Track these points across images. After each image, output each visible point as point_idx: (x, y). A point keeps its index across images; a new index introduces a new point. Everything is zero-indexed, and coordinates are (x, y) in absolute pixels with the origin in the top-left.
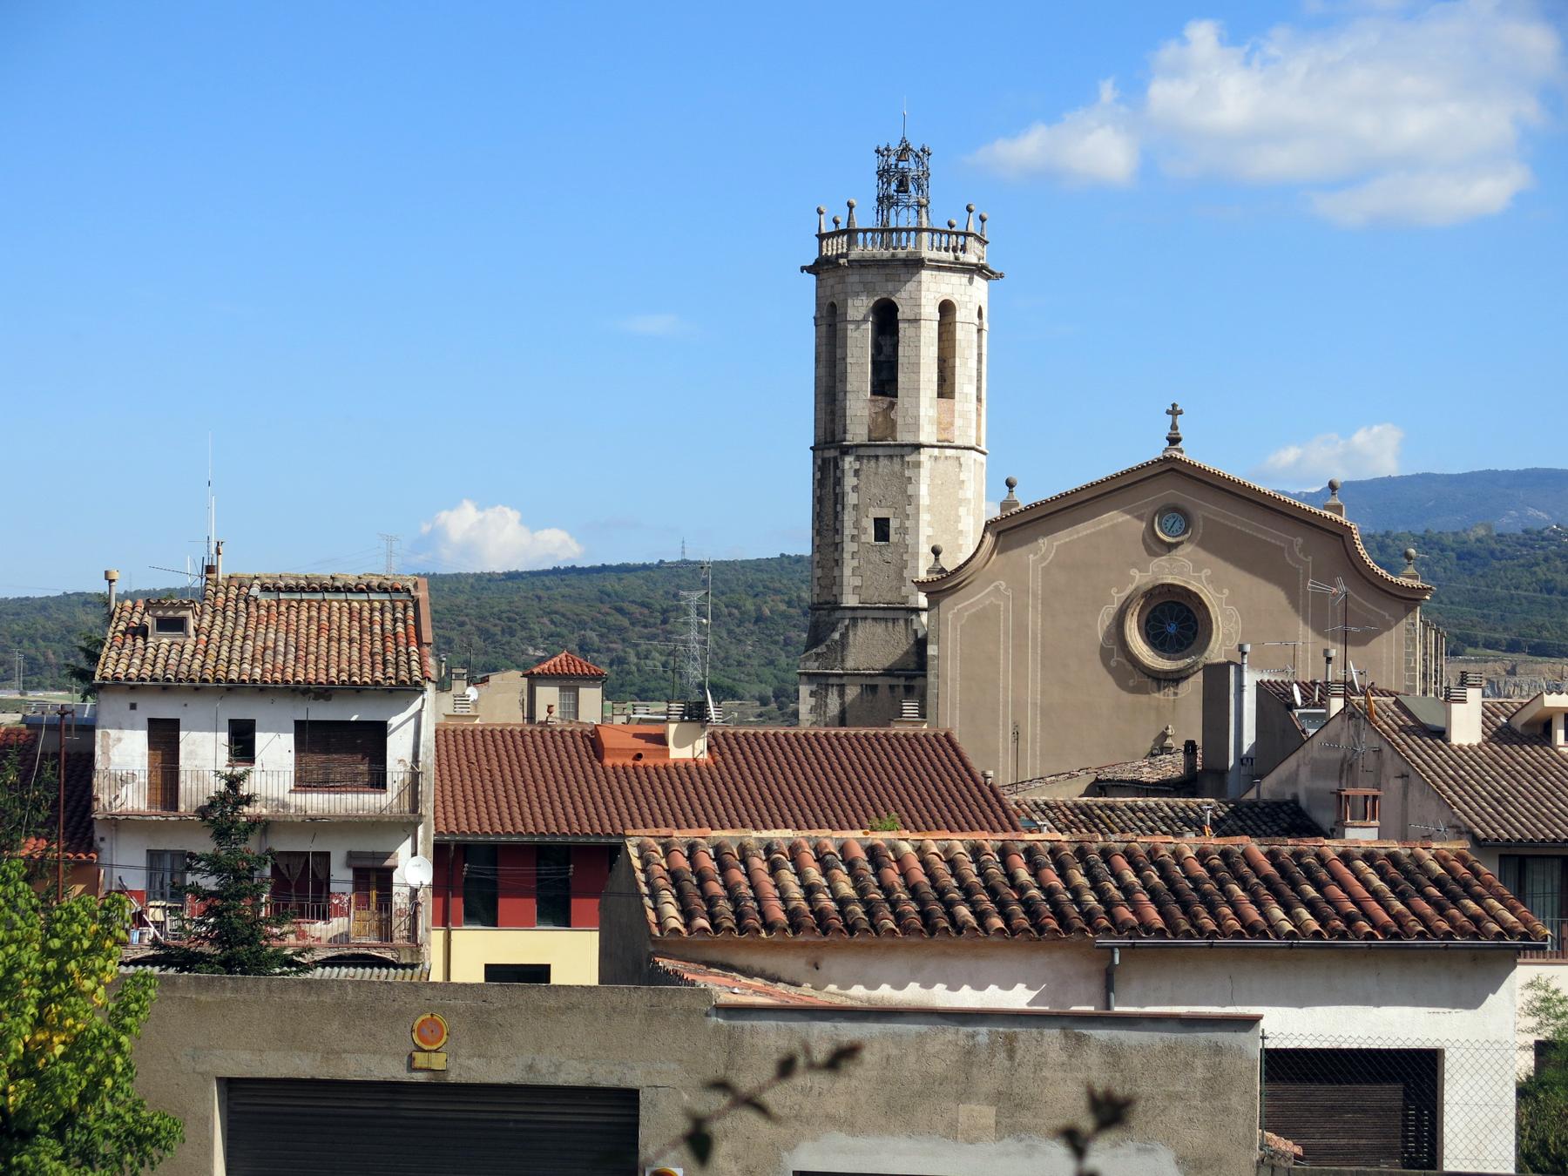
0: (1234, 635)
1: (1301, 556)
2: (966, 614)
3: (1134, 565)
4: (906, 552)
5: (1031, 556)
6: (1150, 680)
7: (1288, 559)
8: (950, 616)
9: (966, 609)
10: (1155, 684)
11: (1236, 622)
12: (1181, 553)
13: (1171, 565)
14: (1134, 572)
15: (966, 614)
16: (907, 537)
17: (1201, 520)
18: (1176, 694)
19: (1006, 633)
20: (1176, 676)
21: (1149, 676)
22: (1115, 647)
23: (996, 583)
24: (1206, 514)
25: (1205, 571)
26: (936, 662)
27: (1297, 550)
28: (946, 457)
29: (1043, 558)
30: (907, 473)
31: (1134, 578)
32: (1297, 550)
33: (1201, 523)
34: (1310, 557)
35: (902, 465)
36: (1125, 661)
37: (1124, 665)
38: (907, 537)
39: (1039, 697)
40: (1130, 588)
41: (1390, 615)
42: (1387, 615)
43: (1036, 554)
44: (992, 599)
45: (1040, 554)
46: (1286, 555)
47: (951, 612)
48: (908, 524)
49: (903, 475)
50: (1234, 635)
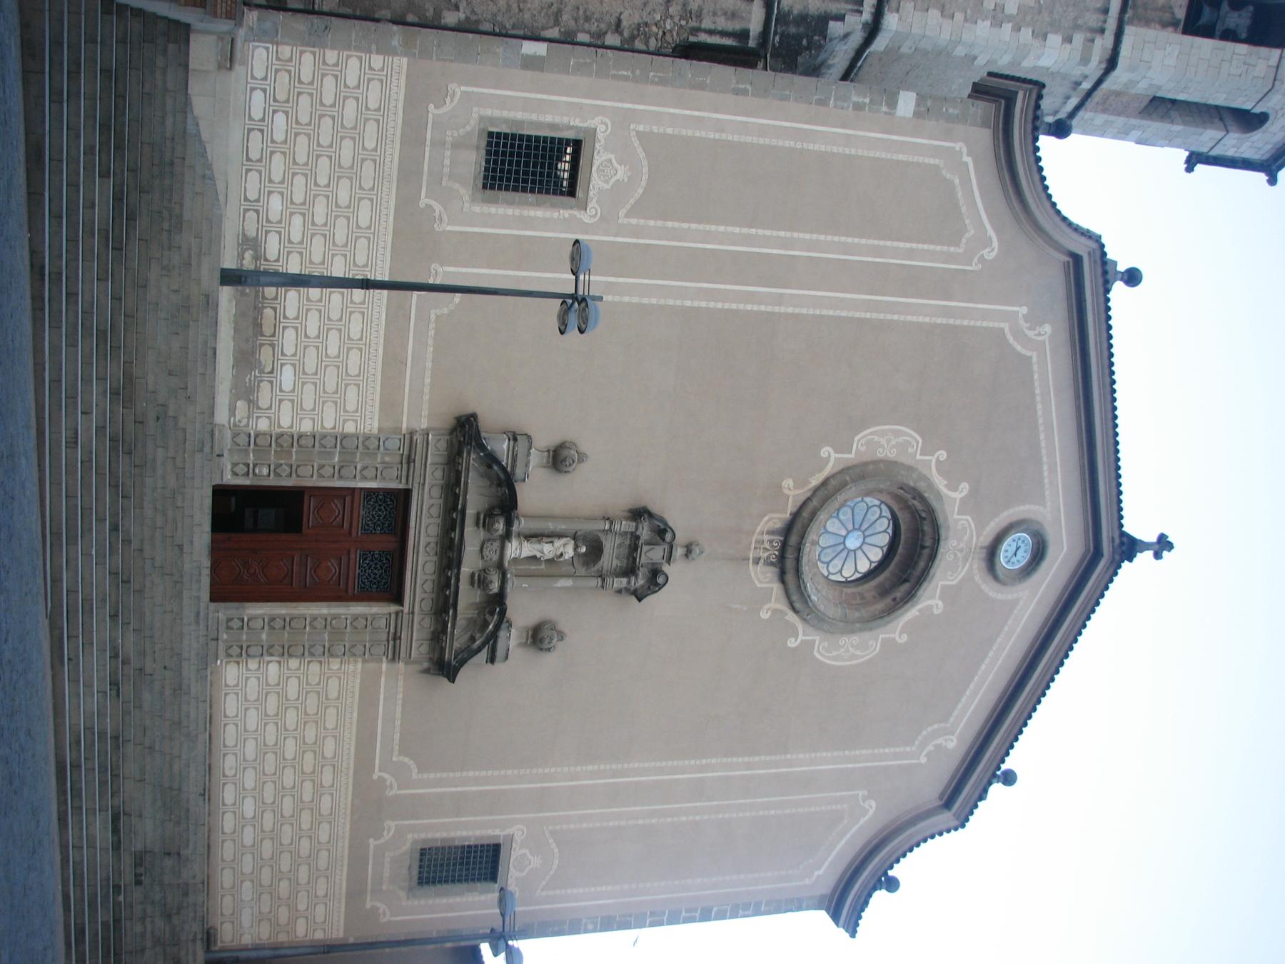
0: (834, 653)
1: (930, 748)
2: (957, 181)
3: (973, 493)
4: (966, 20)
5: (1024, 310)
6: (787, 516)
7: (929, 729)
8: (958, 146)
9: (966, 182)
10: (779, 525)
11: (853, 657)
12: (975, 566)
13: (961, 550)
14: (965, 488)
15: (957, 181)
16: (988, 23)
17: (1015, 596)
18: (757, 561)
19: (910, 254)
20: (790, 564)
21: (796, 516)
22: (852, 456)
23: (995, 244)
24: (1021, 603)
25: (940, 604)
26: (885, 109)
27: (938, 741)
28: (1068, 98)
29: (1018, 333)
30: (1079, 38)
31: (955, 489)
32: (938, 741)
33: (1010, 597)
34: (923, 760)
35: (1093, 30)
36: (827, 471)
37: (820, 470)
38: (988, 23)
39: (790, 310)
40: (940, 483)
41: (819, 876)
42: (821, 872)
43: (1026, 318)
44: (972, 232)
45: (1022, 322)
46: (936, 726)
47: (965, 150)
48: (1007, 27)
49: (1077, 27)
50: (834, 653)
